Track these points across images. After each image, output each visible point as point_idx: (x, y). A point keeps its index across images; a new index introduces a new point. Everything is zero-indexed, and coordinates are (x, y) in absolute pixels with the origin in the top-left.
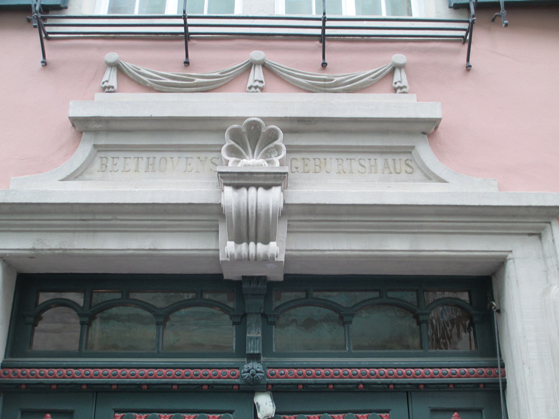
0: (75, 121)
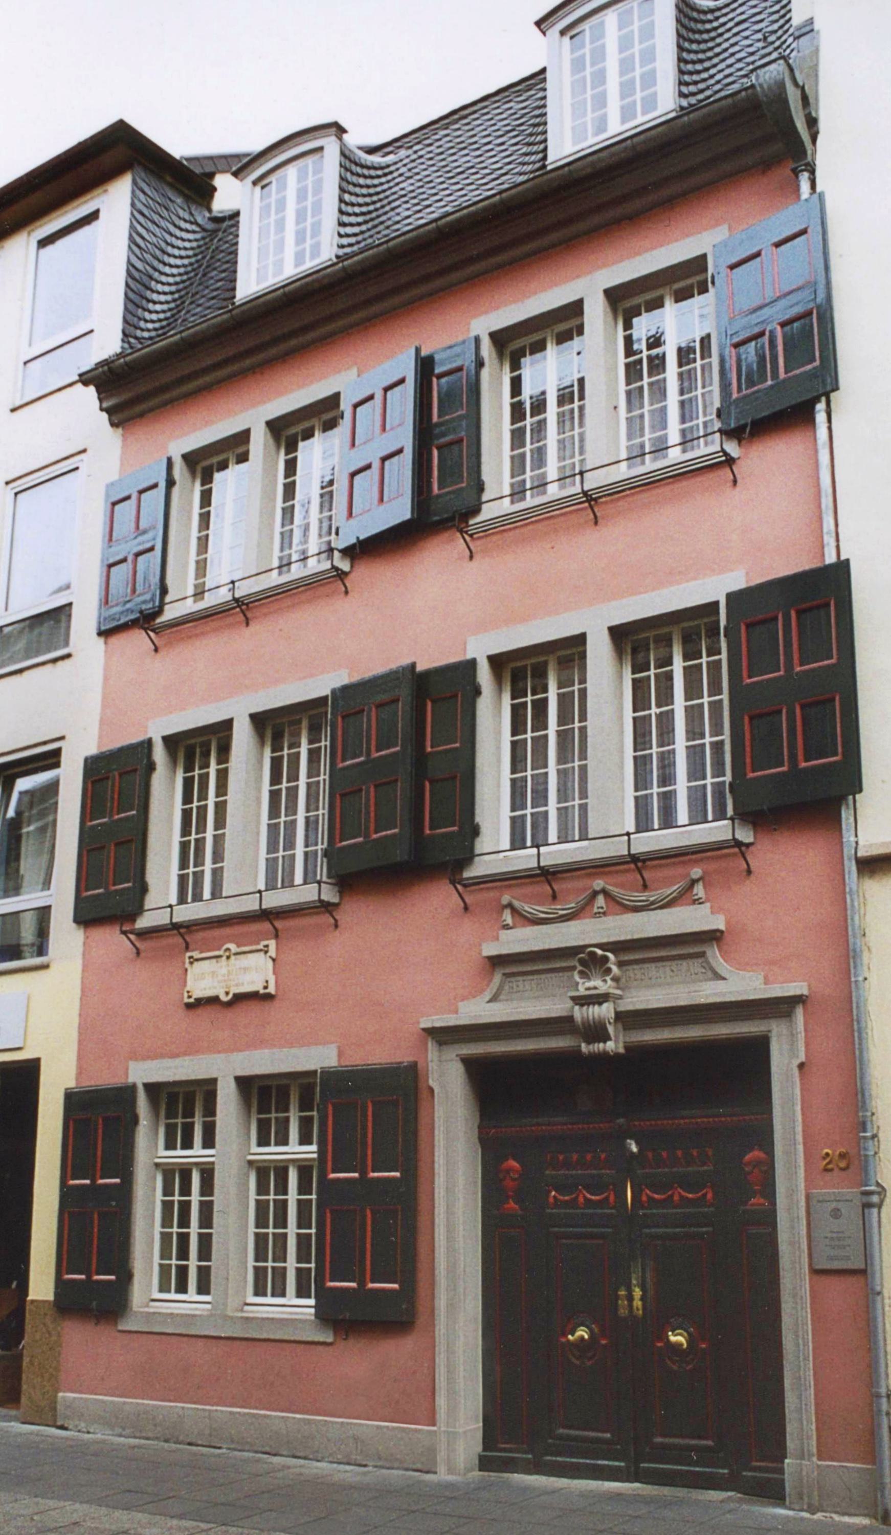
0: (490, 958)
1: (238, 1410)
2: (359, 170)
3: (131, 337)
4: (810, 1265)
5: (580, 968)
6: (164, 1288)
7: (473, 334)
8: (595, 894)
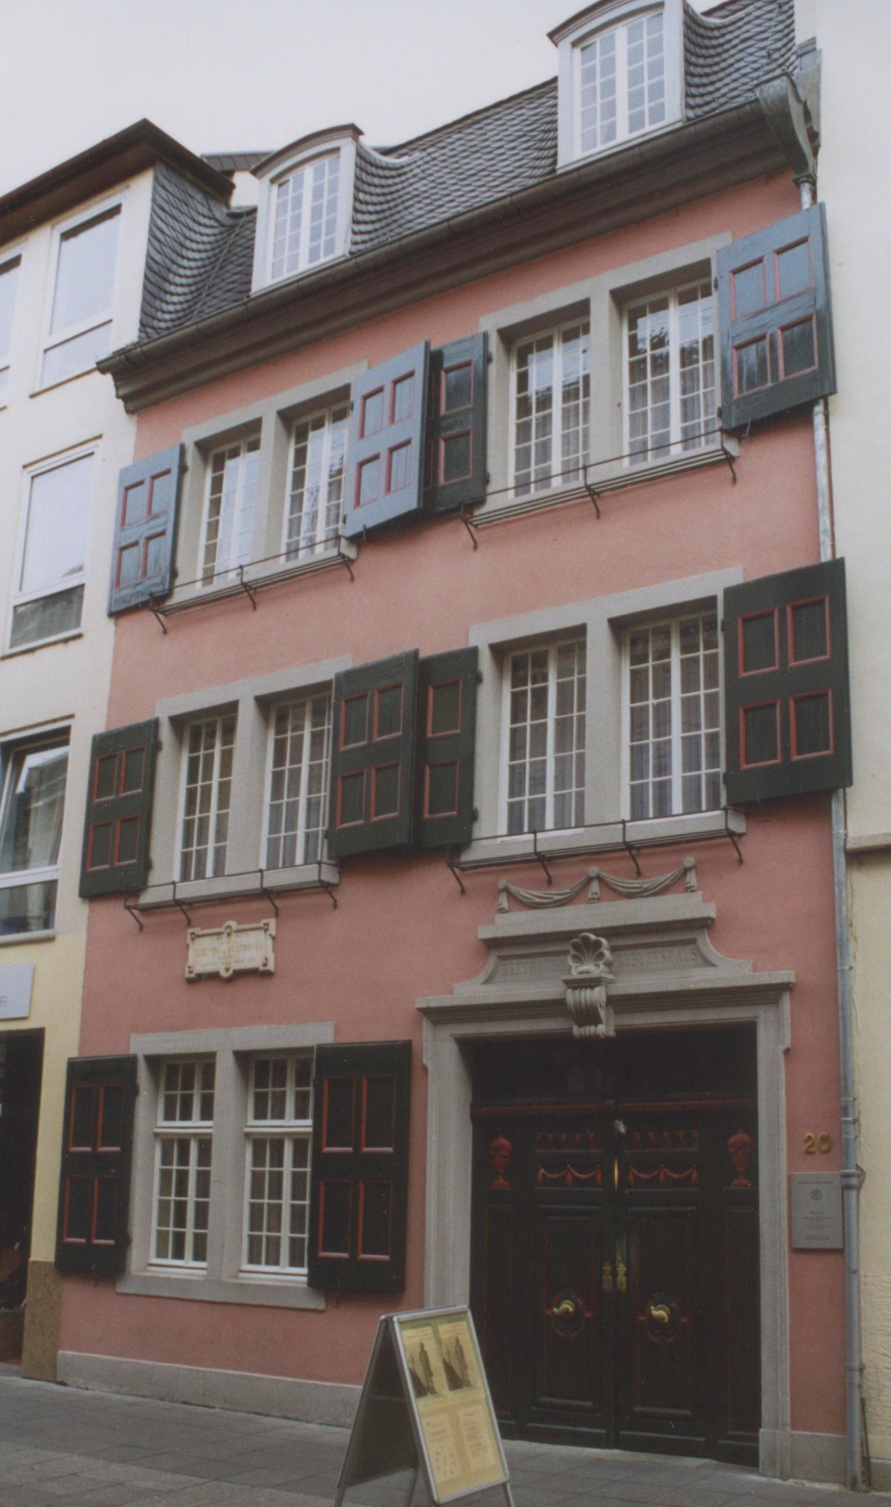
1: (232, 1372)
2: (374, 170)
3: (149, 327)
4: (790, 1244)
5: (573, 952)
6: (161, 1253)
7: (481, 330)
8: (590, 880)
